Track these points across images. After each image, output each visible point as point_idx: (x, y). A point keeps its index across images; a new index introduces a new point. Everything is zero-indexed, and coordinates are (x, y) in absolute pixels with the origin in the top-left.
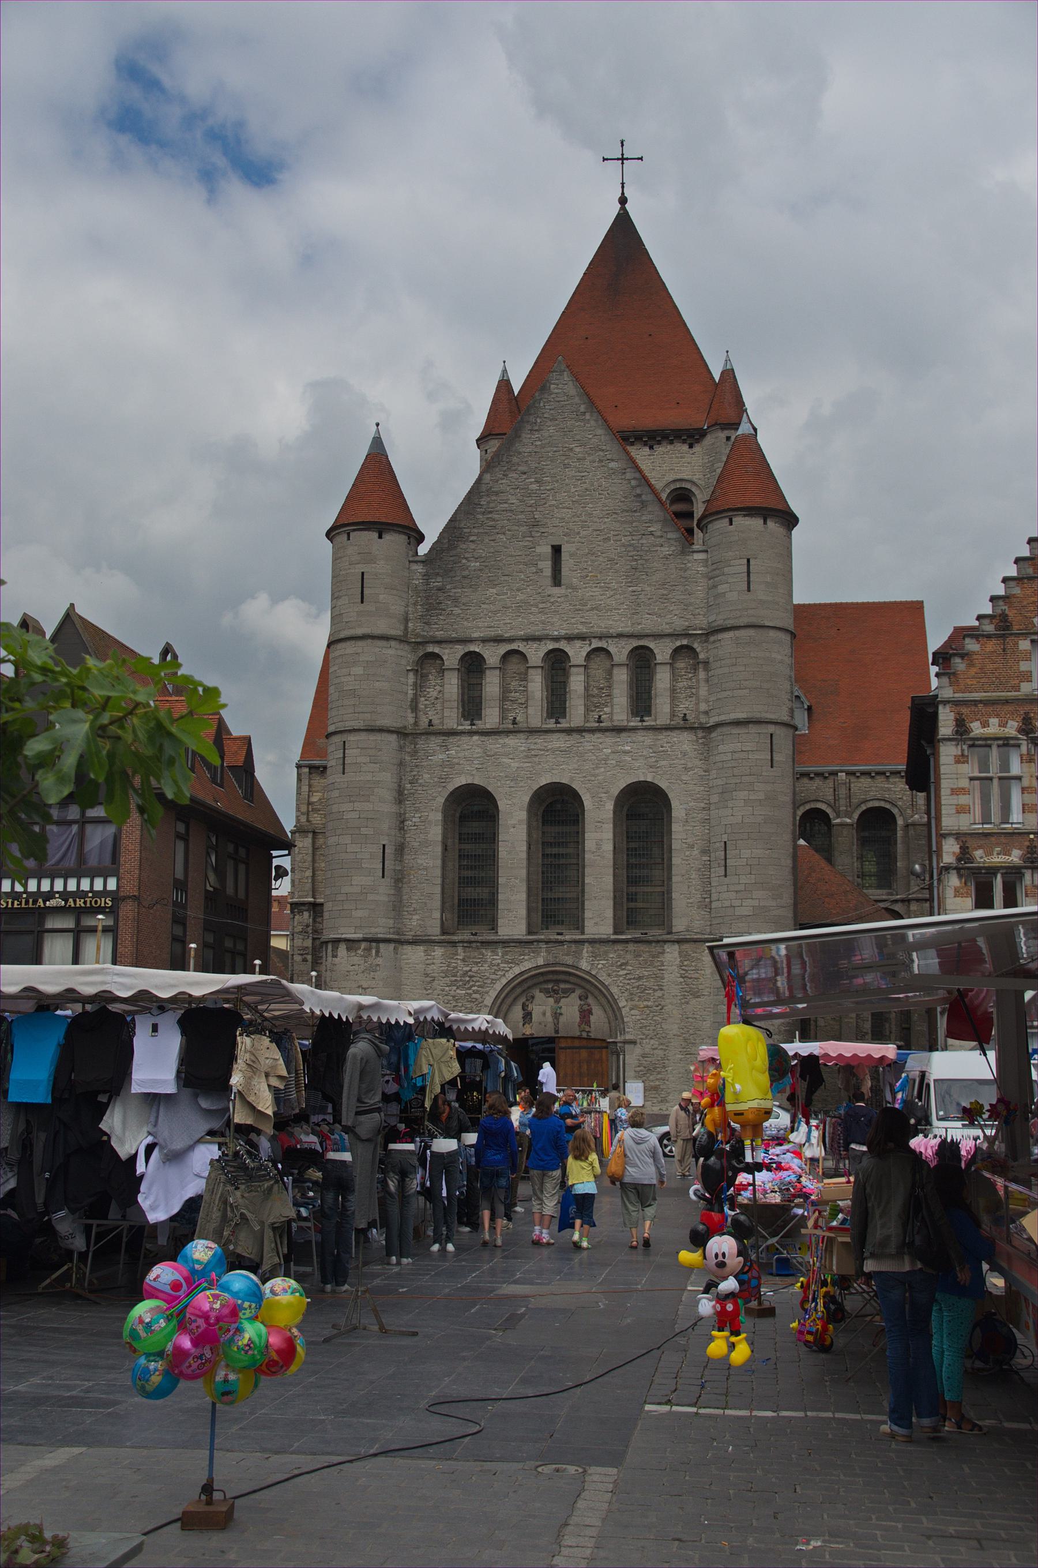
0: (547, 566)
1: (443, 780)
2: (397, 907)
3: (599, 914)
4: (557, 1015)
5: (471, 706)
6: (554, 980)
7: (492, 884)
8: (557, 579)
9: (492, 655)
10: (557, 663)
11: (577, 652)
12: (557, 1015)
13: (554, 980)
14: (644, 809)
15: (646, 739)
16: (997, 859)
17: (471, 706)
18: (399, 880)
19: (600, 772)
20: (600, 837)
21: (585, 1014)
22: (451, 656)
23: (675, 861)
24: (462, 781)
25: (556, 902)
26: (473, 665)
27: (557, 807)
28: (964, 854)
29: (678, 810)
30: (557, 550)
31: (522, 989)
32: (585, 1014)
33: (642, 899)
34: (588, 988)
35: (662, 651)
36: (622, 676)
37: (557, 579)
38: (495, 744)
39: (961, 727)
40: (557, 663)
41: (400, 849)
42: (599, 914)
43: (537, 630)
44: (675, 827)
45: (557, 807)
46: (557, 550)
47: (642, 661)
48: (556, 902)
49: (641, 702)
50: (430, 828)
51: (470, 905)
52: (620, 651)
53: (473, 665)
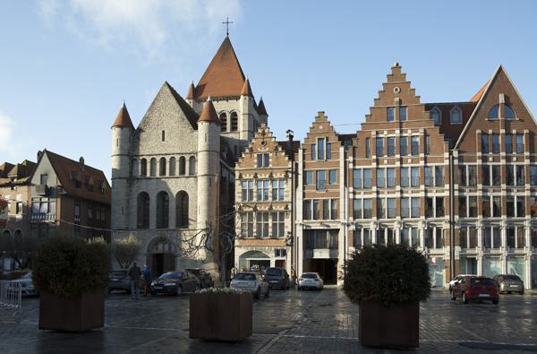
0: (161, 136)
1: (137, 190)
4: (164, 248)
6: (162, 240)
7: (148, 216)
8: (163, 140)
9: (148, 159)
10: (163, 161)
11: (168, 158)
12: (164, 248)
13: (162, 240)
14: (183, 196)
15: (183, 179)
16: (247, 209)
18: (128, 215)
20: (172, 206)
21: (170, 248)
23: (190, 210)
24: (139, 192)
28: (240, 209)
29: (190, 197)
30: (163, 132)
32: (170, 248)
35: (187, 157)
36: (177, 164)
37: (163, 140)
38: (150, 182)
39: (241, 176)
40: (163, 161)
41: (128, 208)
43: (158, 153)
44: (190, 202)
45: (163, 196)
46: (163, 132)
47: (183, 160)
48: (163, 222)
49: (182, 172)
50: (135, 203)
51: (144, 223)
52: (177, 157)
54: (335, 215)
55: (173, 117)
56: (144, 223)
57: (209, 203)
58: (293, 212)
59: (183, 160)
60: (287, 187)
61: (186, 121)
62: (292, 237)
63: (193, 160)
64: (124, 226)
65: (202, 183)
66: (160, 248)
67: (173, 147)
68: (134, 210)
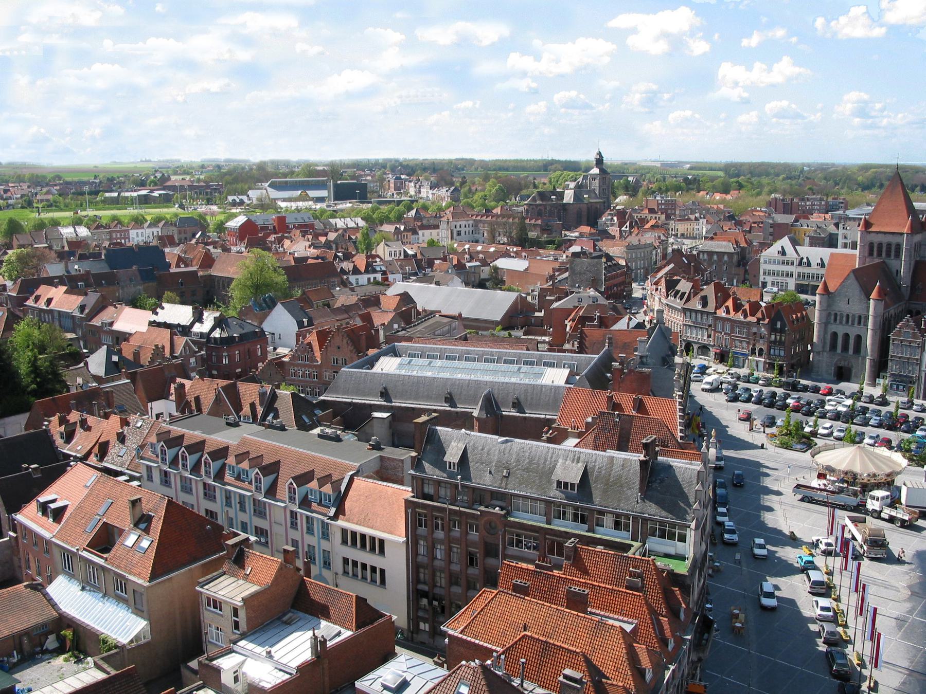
2: (823, 347)
3: (851, 351)
5: (835, 320)
10: (848, 316)
17: (835, 320)
19: (853, 331)
20: (852, 342)
22: (833, 313)
25: (845, 348)
26: (836, 314)
27: (847, 336)
40: (848, 316)
42: (851, 351)
45: (847, 336)
47: (860, 317)
48: (845, 348)
50: (828, 337)
51: (833, 347)
53: (836, 314)
55: (854, 289)
56: (833, 347)
59: (860, 317)
61: (863, 297)
62: (919, 377)
63: (867, 318)
64: (821, 349)
65: (870, 332)
66: (842, 364)
67: (855, 308)
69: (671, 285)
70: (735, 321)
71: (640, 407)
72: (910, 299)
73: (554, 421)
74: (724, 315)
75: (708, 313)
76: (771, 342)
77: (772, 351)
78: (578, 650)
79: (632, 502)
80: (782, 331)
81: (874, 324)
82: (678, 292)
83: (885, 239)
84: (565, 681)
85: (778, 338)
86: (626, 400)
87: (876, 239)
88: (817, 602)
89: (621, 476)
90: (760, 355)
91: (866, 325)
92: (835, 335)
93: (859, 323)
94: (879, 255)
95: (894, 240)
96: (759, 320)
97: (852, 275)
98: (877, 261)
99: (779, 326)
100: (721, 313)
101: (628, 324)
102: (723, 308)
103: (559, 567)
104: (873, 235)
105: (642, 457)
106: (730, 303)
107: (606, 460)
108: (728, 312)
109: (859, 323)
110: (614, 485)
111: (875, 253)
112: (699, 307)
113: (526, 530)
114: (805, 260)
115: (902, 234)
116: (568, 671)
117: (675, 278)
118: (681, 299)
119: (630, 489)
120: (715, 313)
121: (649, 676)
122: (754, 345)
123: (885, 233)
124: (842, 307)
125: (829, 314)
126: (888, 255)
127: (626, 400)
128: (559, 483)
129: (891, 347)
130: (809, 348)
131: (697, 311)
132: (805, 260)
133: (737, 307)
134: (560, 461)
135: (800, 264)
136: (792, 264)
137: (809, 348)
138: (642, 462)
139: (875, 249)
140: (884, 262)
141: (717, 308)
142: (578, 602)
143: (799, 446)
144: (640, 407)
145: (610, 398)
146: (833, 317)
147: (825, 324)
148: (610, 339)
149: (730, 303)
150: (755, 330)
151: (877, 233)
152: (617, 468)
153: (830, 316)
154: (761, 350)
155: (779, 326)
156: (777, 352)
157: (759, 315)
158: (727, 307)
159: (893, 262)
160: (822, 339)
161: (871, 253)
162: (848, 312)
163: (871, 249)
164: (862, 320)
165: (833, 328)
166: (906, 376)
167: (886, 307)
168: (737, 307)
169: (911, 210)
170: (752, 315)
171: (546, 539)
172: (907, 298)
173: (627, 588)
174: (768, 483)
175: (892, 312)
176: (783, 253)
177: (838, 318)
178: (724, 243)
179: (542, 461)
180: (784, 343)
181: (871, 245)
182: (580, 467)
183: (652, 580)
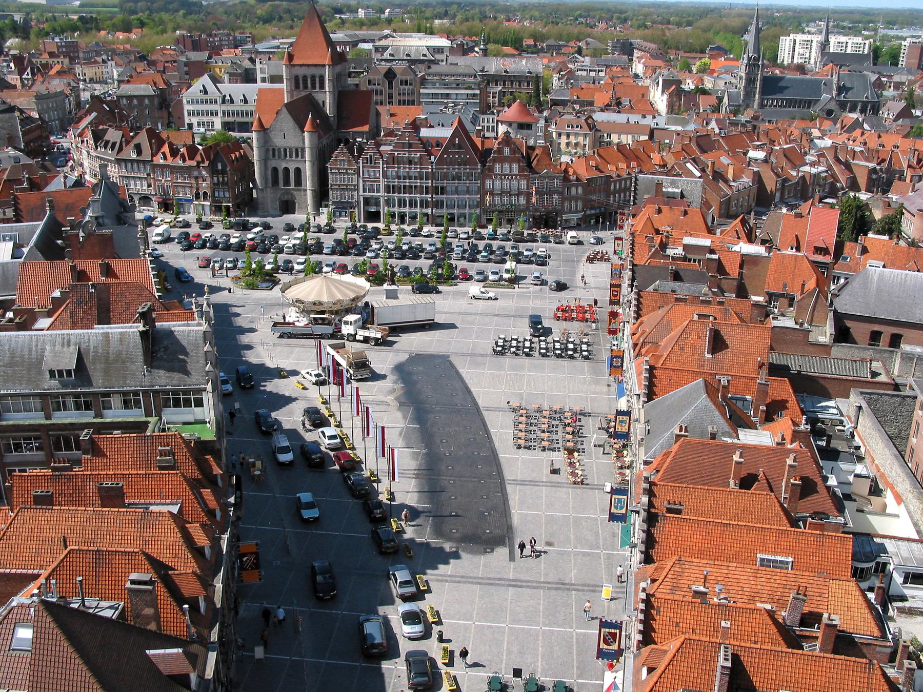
2: (266, 183)
5: (274, 155)
10: (285, 150)
14: (298, 171)
17: (274, 155)
19: (292, 167)
22: (271, 149)
26: (274, 150)
31: (283, 194)
33: (299, 182)
34: (292, 195)
40: (285, 150)
45: (286, 170)
47: (297, 150)
48: (287, 182)
50: (269, 173)
53: (274, 150)
54: (378, 191)
55: (287, 122)
56: (275, 182)
57: (313, 176)
58: (358, 190)
59: (297, 150)
60: (355, 177)
61: (297, 129)
62: (358, 202)
63: (303, 150)
67: (291, 142)
68: (270, 177)
69: (98, 137)
70: (174, 167)
71: (108, 271)
72: (338, 128)
73: (13, 302)
74: (162, 162)
75: (144, 162)
76: (214, 184)
77: (216, 194)
78: (136, 550)
79: (140, 377)
80: (223, 172)
81: (312, 155)
82: (107, 142)
83: (309, 72)
84: (133, 586)
85: (221, 179)
86: (92, 268)
87: (301, 72)
88: (323, 433)
89: (120, 352)
90: (205, 198)
91: (303, 156)
92: (275, 170)
93: (297, 156)
94: (306, 87)
95: (316, 72)
96: (199, 163)
97: (284, 110)
98: (303, 94)
99: (220, 167)
100: (159, 160)
101: (65, 183)
102: (160, 155)
103: (78, 462)
104: (297, 68)
105: (141, 328)
106: (166, 149)
107: (100, 337)
108: (165, 158)
109: (297, 156)
110: (114, 361)
111: (301, 86)
112: (134, 156)
113: (23, 431)
114: (228, 98)
115: (324, 66)
116: (134, 576)
117: (101, 127)
118: (113, 148)
119: (133, 363)
120: (152, 161)
121: (207, 552)
122: (198, 189)
123: (308, 66)
124: (278, 141)
125: (268, 150)
126: (314, 87)
127: (92, 268)
128: (52, 373)
129: (330, 176)
130: (251, 186)
131: (132, 161)
132: (228, 98)
133: (174, 152)
134: (48, 348)
135: (224, 102)
136: (216, 102)
137: (251, 186)
138: (142, 333)
139: (301, 82)
140: (310, 94)
141: (153, 155)
142: (112, 497)
143: (264, 285)
144: (108, 271)
145: (73, 268)
146: (271, 153)
147: (264, 161)
148: (50, 202)
149: (166, 149)
150: (196, 173)
151: (301, 66)
152: (114, 345)
153: (270, 152)
154: (205, 193)
155: (220, 167)
156: (221, 194)
157: (198, 158)
158: (164, 154)
159: (319, 97)
160: (264, 177)
161: (297, 87)
162: (285, 145)
163: (297, 82)
164: (299, 152)
165: (273, 163)
166: (347, 202)
167: (320, 137)
168: (174, 152)
169: (330, 43)
170: (191, 158)
171: (49, 436)
172: (335, 127)
173: (161, 468)
174: (240, 322)
175: (325, 142)
176: (205, 92)
177: (276, 153)
178: (142, 86)
179: (26, 352)
180: (227, 184)
181: (296, 78)
182: (73, 350)
183: (183, 454)
